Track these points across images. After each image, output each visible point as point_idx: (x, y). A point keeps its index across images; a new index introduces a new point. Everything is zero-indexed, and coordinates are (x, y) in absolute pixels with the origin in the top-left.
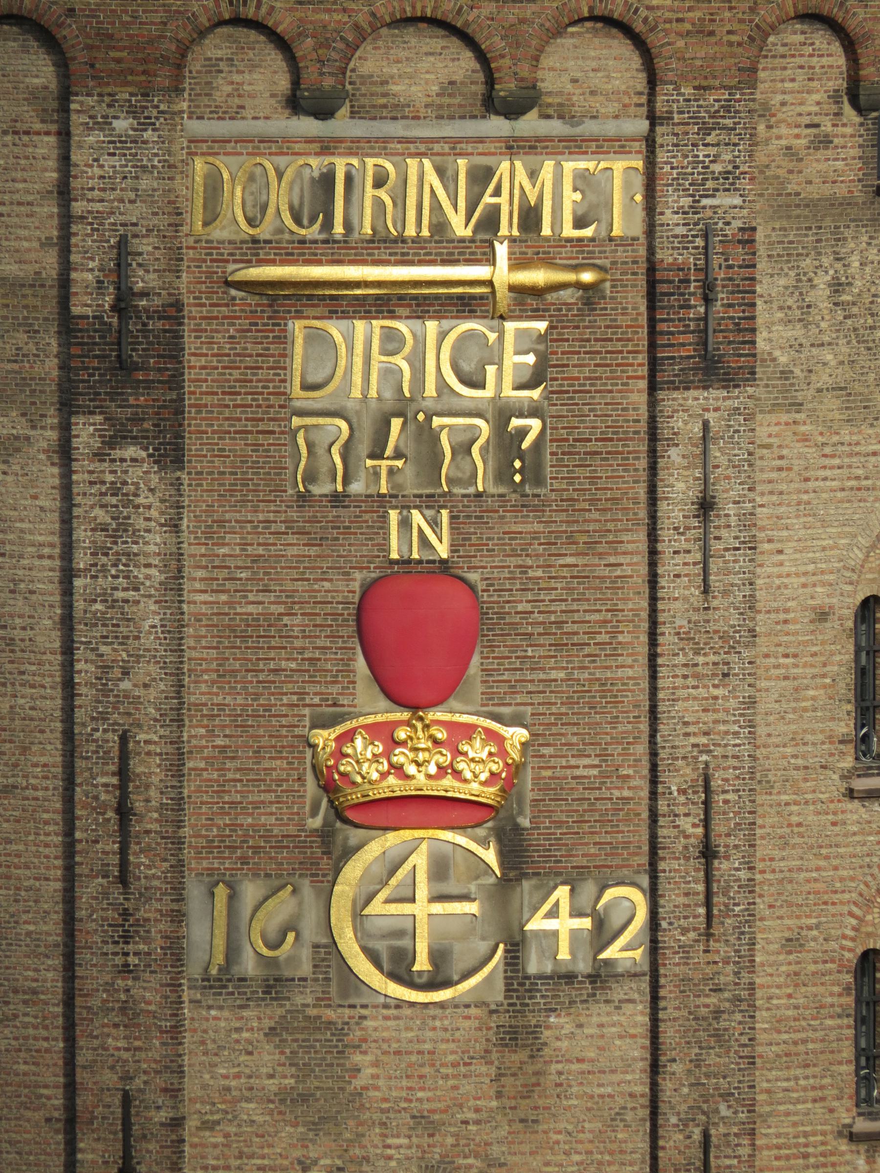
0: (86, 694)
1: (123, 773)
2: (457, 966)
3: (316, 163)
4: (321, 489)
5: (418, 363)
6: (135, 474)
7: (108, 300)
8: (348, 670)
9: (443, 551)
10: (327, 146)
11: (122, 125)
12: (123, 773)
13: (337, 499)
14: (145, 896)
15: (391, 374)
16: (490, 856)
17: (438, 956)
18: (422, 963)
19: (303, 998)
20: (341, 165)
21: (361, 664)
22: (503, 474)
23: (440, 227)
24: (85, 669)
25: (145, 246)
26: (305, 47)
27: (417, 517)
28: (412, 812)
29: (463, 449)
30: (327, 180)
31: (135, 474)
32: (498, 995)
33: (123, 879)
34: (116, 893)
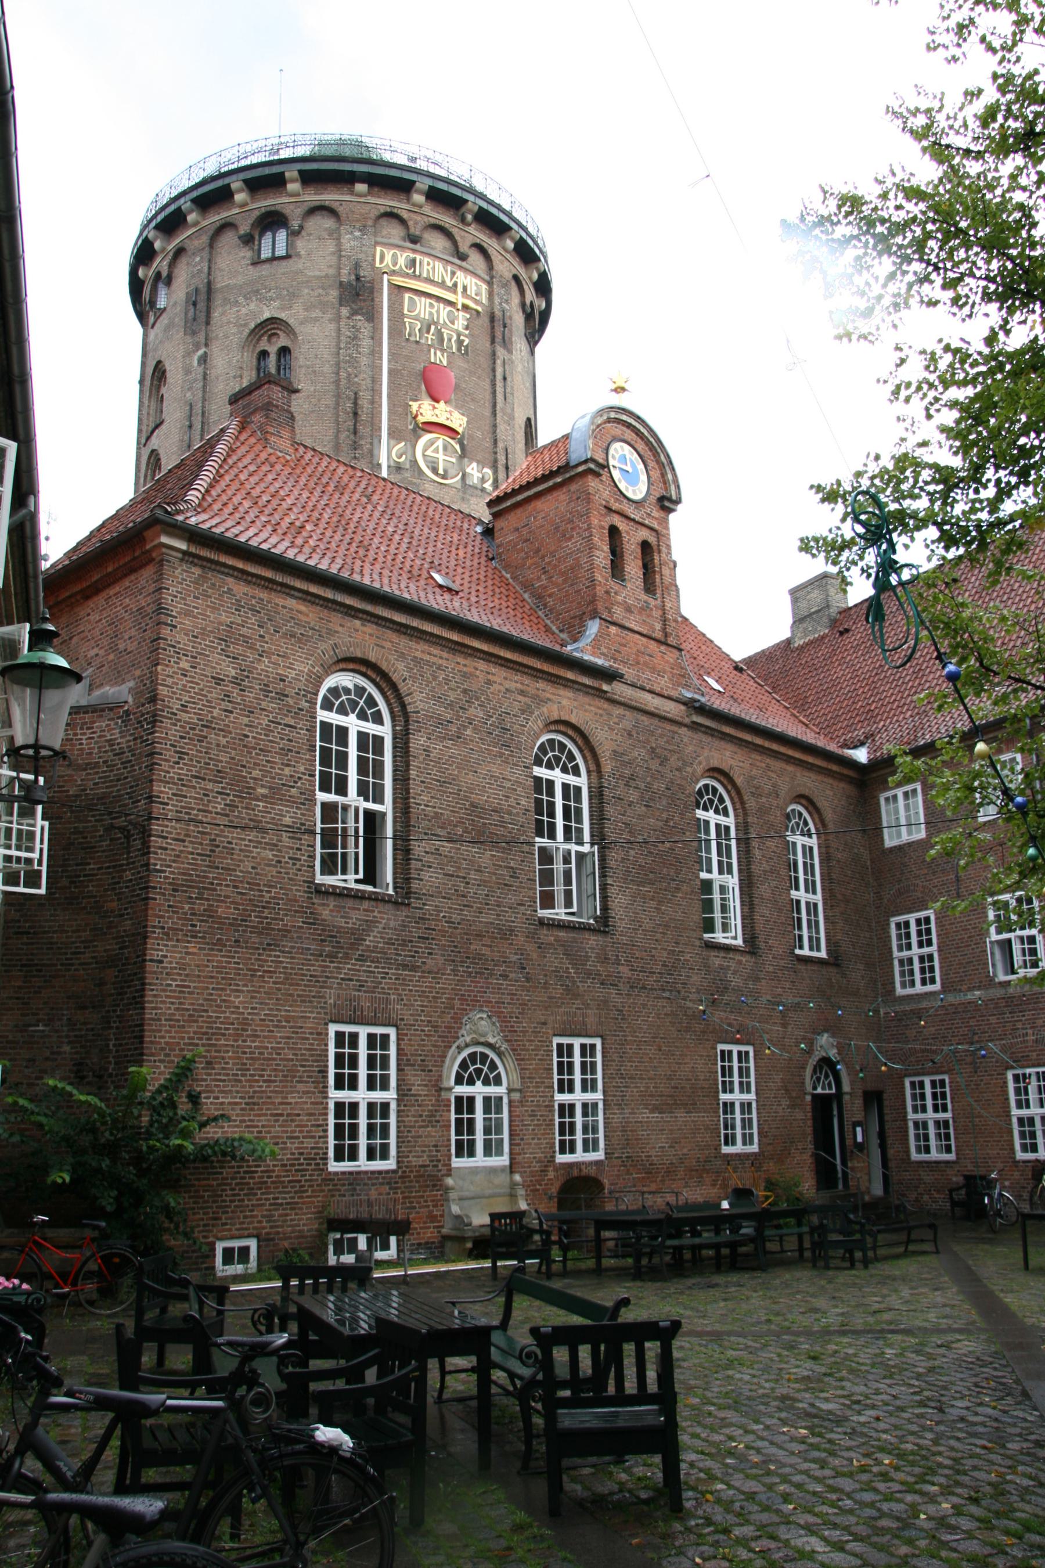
0: (343, 382)
1: (355, 403)
2: (450, 475)
3: (412, 255)
4: (412, 339)
5: (438, 312)
6: (359, 324)
7: (353, 277)
8: (419, 387)
9: (445, 363)
10: (414, 251)
11: (357, 234)
12: (355, 403)
13: (417, 342)
14: (361, 438)
15: (431, 314)
16: (458, 447)
17: (445, 471)
18: (441, 471)
19: (407, 475)
20: (418, 257)
21: (423, 387)
22: (459, 349)
23: (444, 282)
24: (343, 375)
25: (364, 265)
26: (411, 223)
27: (439, 353)
28: (438, 429)
29: (450, 340)
30: (414, 261)
31: (359, 324)
32: (459, 486)
33: (355, 432)
34: (352, 437)
